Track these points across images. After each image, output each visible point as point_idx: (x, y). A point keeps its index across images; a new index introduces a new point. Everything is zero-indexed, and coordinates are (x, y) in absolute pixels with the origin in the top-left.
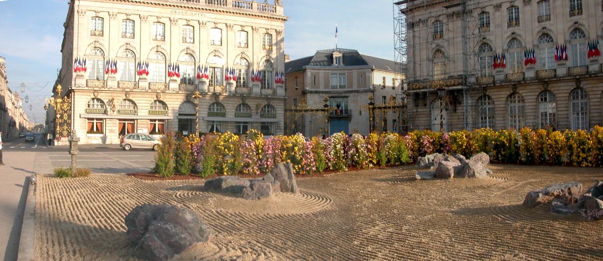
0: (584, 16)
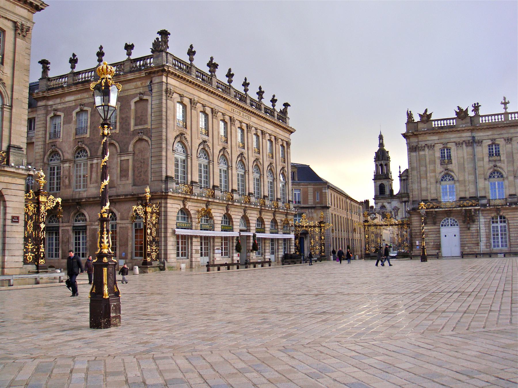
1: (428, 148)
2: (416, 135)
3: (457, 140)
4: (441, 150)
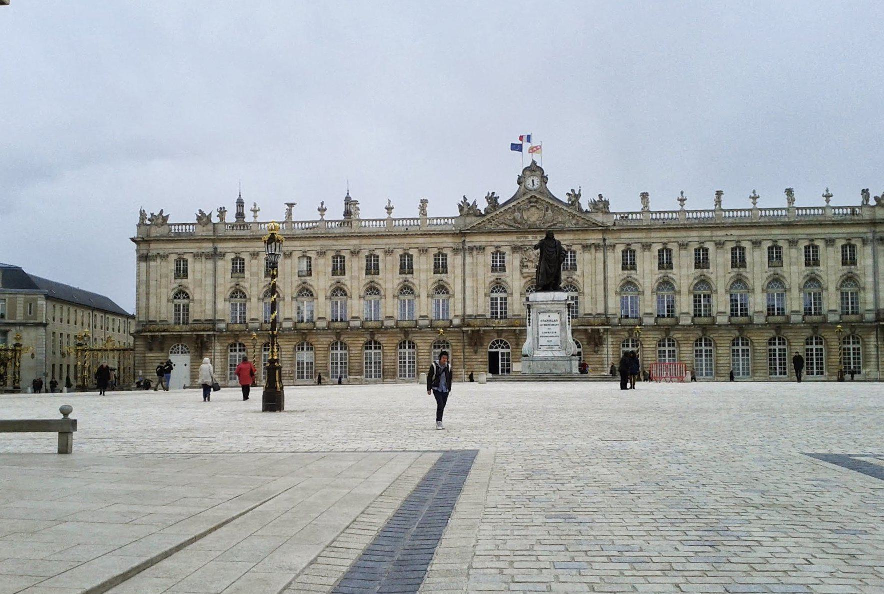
0: (347, 277)
1: (161, 258)
2: (146, 241)
3: (194, 251)
4: (177, 262)
